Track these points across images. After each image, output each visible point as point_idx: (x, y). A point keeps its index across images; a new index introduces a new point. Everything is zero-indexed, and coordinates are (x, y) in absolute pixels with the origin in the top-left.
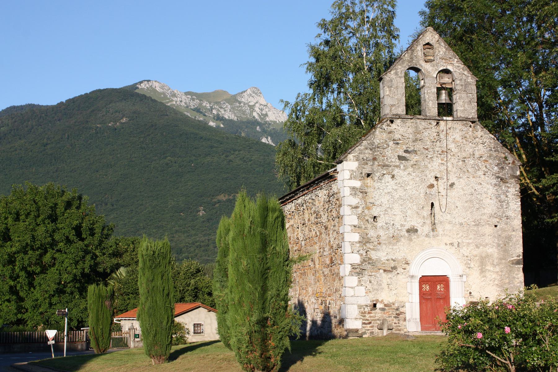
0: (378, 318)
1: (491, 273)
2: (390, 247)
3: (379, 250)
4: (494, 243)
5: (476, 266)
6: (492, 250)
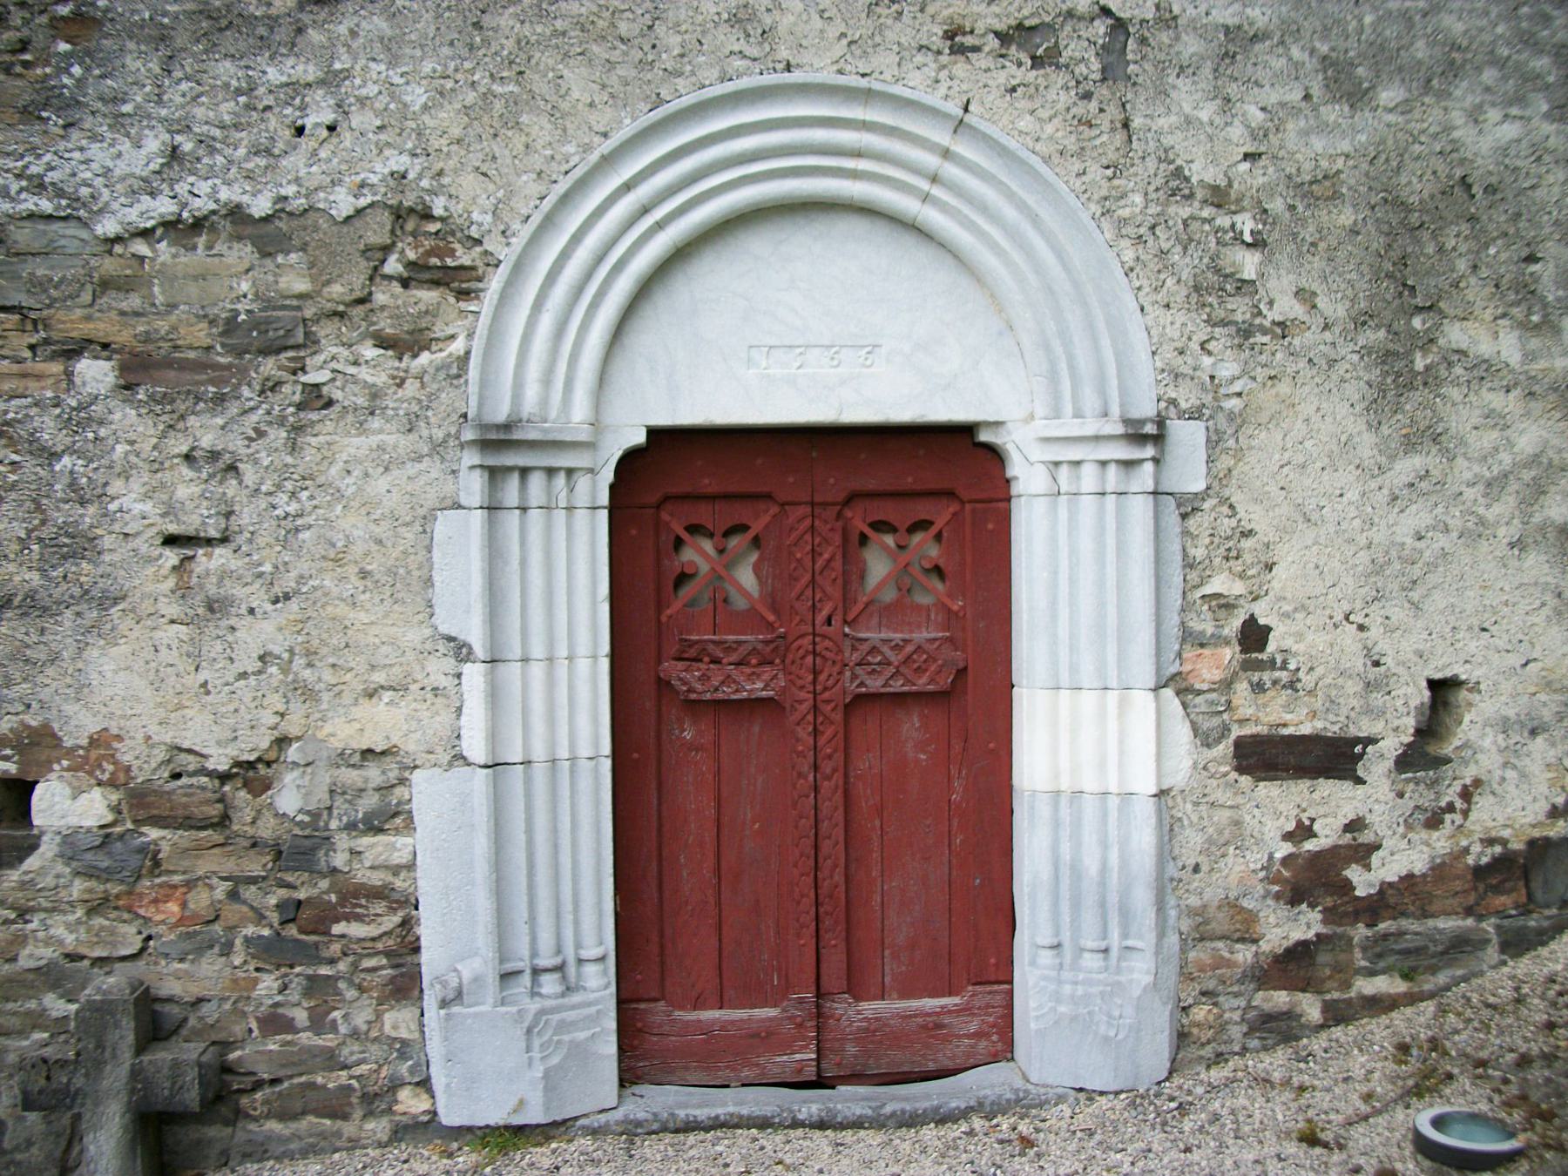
0: (48, 953)
1: (1496, 400)
2: (226, 70)
3: (69, 106)
4: (1537, 47)
5: (1333, 307)
6: (1510, 131)
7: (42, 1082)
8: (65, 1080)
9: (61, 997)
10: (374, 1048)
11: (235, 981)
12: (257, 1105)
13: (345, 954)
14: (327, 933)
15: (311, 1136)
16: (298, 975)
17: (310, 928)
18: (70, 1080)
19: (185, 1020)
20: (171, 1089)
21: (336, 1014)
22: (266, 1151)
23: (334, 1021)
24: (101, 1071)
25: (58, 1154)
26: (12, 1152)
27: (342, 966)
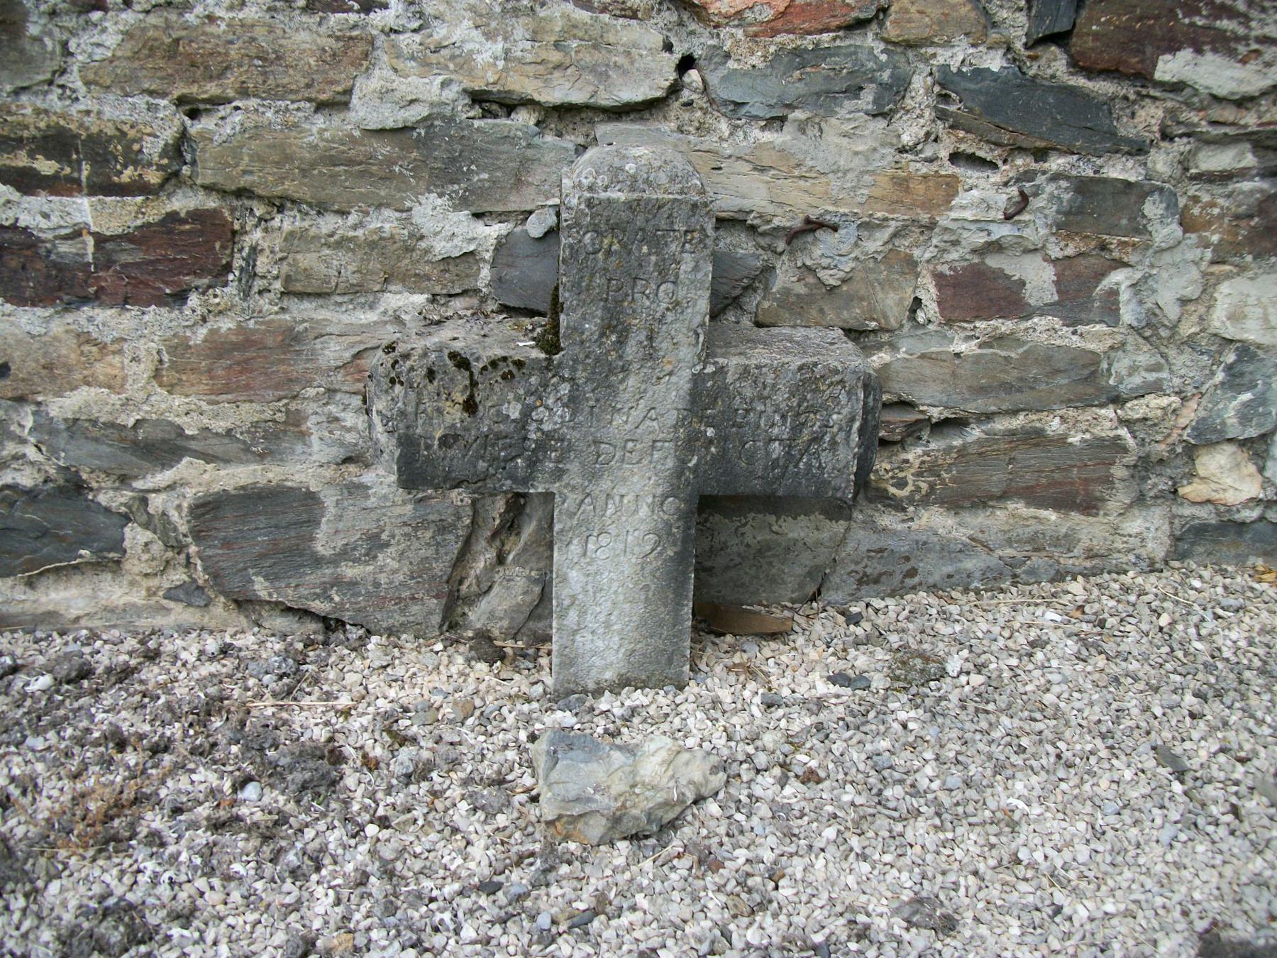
7: (455, 415)
8: (514, 411)
9: (462, 203)
10: (1182, 361)
11: (902, 183)
12: (909, 475)
13: (1166, 136)
14: (1143, 77)
15: (1009, 542)
16: (1056, 177)
17: (1106, 60)
18: (527, 413)
19: (768, 270)
20: (789, 444)
21: (1119, 278)
22: (912, 573)
23: (1113, 293)
24: (613, 390)
25: (440, 567)
26: (335, 560)
27: (1162, 161)
